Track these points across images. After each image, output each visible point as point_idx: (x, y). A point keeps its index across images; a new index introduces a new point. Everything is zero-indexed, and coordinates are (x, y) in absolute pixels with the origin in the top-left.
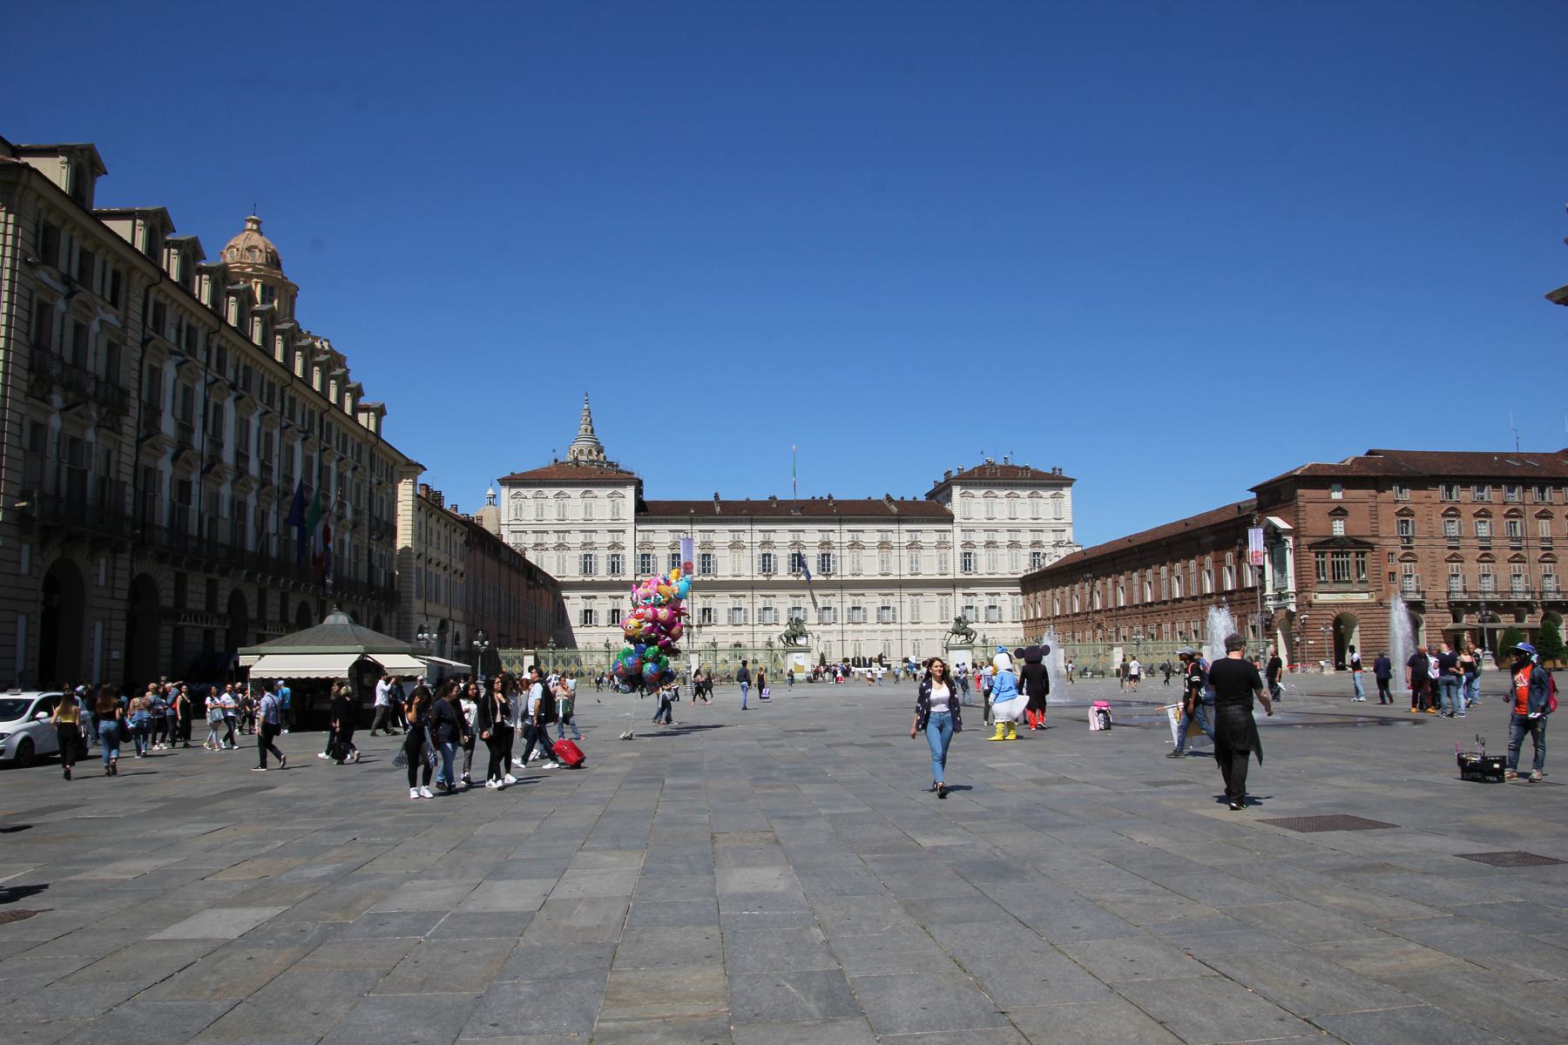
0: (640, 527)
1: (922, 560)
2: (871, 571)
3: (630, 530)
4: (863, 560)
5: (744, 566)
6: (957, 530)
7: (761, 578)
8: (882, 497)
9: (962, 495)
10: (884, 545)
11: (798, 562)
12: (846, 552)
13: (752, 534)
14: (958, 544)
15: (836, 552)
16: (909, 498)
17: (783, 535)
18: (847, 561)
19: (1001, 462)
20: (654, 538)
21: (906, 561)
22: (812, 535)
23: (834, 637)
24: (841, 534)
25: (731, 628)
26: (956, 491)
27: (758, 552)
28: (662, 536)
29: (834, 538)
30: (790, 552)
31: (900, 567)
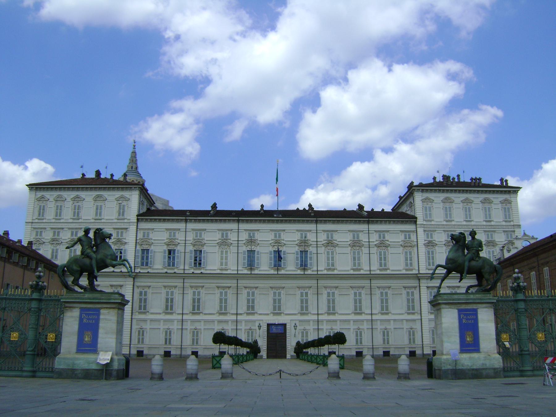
0: (143, 225)
1: (390, 257)
2: (344, 265)
3: (133, 228)
4: (337, 257)
5: (234, 264)
6: (420, 231)
7: (246, 272)
8: (355, 208)
9: (423, 201)
10: (356, 244)
11: (278, 257)
12: (322, 250)
13: (239, 232)
14: (421, 242)
15: (312, 249)
16: (378, 209)
17: (265, 233)
18: (323, 258)
20: (153, 236)
21: (375, 258)
22: (291, 233)
23: (311, 327)
24: (316, 233)
25: (216, 317)
26: (418, 197)
27: (244, 249)
28: (159, 232)
29: (311, 237)
30: (272, 249)
31: (370, 263)
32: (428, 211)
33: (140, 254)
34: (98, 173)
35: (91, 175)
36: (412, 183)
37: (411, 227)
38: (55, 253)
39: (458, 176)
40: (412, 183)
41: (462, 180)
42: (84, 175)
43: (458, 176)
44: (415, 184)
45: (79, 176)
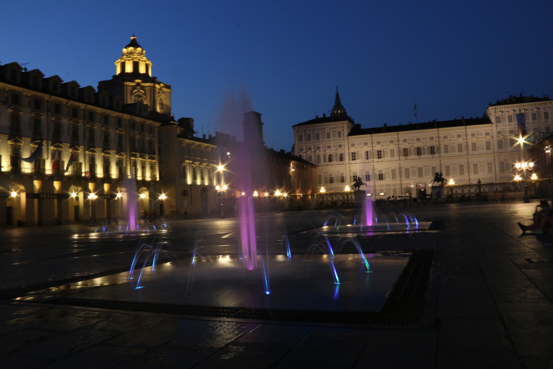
3: (346, 142)
16: (474, 117)
19: (518, 96)
32: (498, 120)
33: (351, 155)
34: (324, 115)
35: (321, 116)
36: (491, 103)
37: (490, 128)
38: (310, 157)
39: (521, 94)
40: (491, 103)
41: (523, 96)
42: (317, 116)
43: (521, 94)
44: (492, 104)
45: (315, 118)
